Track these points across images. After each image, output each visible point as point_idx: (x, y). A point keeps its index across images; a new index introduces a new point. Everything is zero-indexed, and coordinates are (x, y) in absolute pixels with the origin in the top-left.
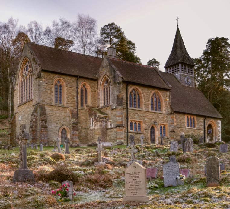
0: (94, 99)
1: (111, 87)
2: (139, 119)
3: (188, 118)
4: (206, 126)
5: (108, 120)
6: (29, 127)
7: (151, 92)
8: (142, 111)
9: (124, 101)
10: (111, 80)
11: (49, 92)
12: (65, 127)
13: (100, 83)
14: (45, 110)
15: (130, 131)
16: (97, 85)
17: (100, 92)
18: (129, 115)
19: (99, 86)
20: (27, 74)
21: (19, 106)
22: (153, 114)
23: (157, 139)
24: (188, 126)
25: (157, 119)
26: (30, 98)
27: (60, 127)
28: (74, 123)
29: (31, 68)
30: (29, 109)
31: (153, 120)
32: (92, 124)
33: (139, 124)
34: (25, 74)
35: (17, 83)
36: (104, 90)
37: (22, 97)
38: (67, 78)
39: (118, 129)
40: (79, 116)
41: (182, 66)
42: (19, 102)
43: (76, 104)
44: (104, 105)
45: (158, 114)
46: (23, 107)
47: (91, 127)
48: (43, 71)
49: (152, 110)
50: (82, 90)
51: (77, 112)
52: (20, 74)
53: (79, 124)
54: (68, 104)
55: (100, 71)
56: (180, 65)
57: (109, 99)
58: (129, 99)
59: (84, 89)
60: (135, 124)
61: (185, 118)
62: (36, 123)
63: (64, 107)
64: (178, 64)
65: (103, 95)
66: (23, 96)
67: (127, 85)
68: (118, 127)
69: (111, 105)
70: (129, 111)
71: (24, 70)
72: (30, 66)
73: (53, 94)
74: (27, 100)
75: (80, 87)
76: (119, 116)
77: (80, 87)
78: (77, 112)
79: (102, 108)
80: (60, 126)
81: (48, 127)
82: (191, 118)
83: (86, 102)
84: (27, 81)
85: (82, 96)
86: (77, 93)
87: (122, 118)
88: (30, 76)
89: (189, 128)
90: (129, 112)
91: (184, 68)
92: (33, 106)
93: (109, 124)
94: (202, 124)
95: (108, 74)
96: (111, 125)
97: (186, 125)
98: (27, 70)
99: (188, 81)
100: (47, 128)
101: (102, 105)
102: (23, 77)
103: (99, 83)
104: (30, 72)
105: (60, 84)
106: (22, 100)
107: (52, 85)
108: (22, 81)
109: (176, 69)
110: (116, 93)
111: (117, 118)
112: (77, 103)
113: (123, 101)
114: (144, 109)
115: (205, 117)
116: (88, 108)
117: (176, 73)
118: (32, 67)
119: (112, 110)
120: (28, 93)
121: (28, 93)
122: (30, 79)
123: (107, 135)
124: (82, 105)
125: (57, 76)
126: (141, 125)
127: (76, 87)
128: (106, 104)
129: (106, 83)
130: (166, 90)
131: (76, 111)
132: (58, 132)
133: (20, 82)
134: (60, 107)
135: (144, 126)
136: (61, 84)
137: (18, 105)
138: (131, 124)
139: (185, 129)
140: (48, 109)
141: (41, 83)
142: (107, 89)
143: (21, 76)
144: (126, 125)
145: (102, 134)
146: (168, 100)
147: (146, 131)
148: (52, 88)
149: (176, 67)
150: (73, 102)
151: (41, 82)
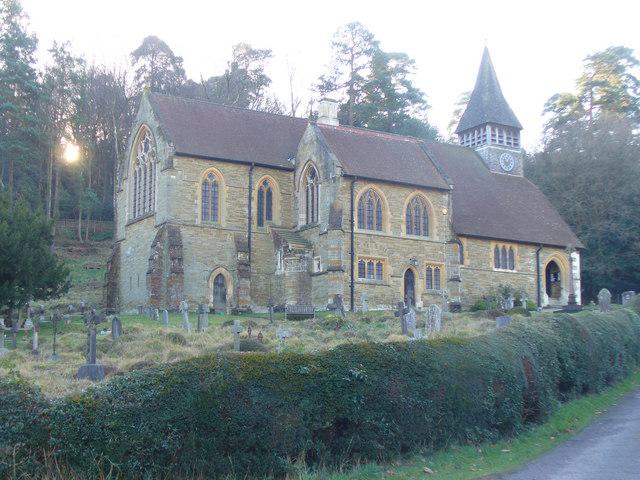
0: (290, 209)
3: (497, 251)
4: (543, 267)
5: (314, 255)
7: (406, 197)
9: (345, 217)
12: (223, 271)
14: (180, 237)
15: (357, 278)
17: (298, 195)
18: (355, 246)
19: (297, 183)
23: (418, 297)
25: (420, 253)
28: (241, 263)
30: (146, 232)
31: (411, 256)
33: (379, 265)
34: (143, 157)
38: (230, 168)
41: (493, 130)
46: (136, 227)
48: (178, 154)
49: (408, 233)
50: (260, 192)
51: (249, 238)
53: (252, 265)
55: (300, 152)
56: (489, 129)
57: (315, 212)
58: (356, 213)
59: (265, 189)
60: (370, 264)
61: (489, 248)
62: (161, 264)
64: (484, 126)
71: (139, 150)
73: (199, 201)
76: (332, 249)
77: (256, 187)
78: (249, 238)
79: (304, 228)
82: (504, 249)
83: (269, 217)
85: (260, 203)
86: (250, 198)
87: (340, 253)
89: (500, 270)
92: (156, 227)
93: (315, 263)
94: (533, 261)
95: (314, 159)
97: (492, 265)
98: (146, 151)
99: (507, 164)
101: (302, 223)
104: (153, 154)
110: (329, 200)
112: (250, 218)
113: (344, 217)
114: (390, 233)
115: (539, 246)
116: (273, 231)
118: (155, 146)
123: (311, 287)
124: (260, 223)
128: (310, 221)
129: (312, 178)
130: (443, 191)
133: (131, 174)
135: (388, 269)
138: (361, 265)
140: (186, 234)
142: (313, 189)
144: (348, 266)
145: (300, 286)
146: (445, 211)
147: (395, 279)
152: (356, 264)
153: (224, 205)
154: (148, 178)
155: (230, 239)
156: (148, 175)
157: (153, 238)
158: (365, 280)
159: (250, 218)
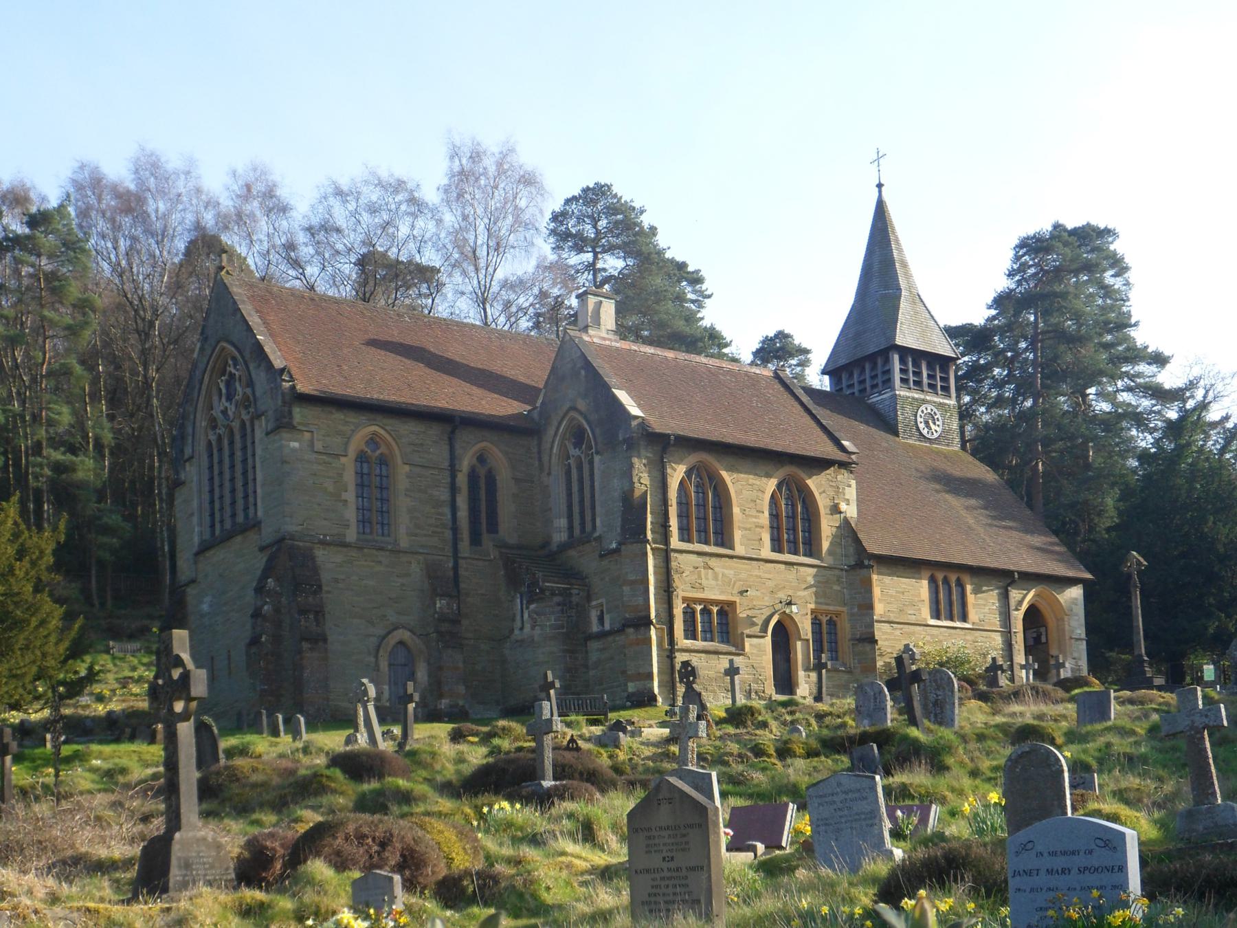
1: (597, 458)
2: (722, 593)
4: (1018, 616)
6: (247, 641)
8: (731, 557)
10: (598, 431)
11: (331, 488)
12: (405, 635)
13: (549, 446)
14: (315, 570)
15: (682, 641)
16: (539, 453)
19: (545, 458)
20: (230, 413)
21: (197, 554)
22: (783, 566)
24: (938, 617)
26: (246, 517)
27: (384, 638)
28: (443, 619)
29: (248, 386)
31: (782, 595)
32: (518, 617)
33: (722, 613)
35: (188, 451)
36: (568, 473)
37: (212, 515)
38: (408, 429)
39: (632, 637)
40: (462, 585)
42: (201, 533)
43: (448, 534)
44: (571, 535)
45: (802, 569)
46: (218, 555)
47: (517, 632)
50: (473, 477)
51: (456, 568)
52: (198, 416)
53: (465, 622)
54: (416, 535)
59: (482, 472)
60: (706, 611)
63: (399, 552)
65: (563, 495)
66: (217, 506)
67: (664, 450)
68: (631, 630)
69: (600, 537)
70: (678, 561)
71: (215, 398)
72: (244, 379)
74: (234, 524)
75: (465, 464)
76: (633, 583)
77: (465, 464)
78: (456, 568)
79: (564, 547)
80: (381, 632)
81: (330, 639)
83: (493, 527)
84: (232, 443)
86: (454, 489)
88: (243, 423)
90: (673, 564)
91: (911, 369)
92: (262, 549)
93: (594, 615)
96: (601, 619)
97: (925, 613)
98: (229, 399)
100: (325, 640)
101: (560, 537)
102: (214, 428)
103: (546, 446)
105: (378, 452)
106: (213, 526)
107: (343, 460)
108: (210, 443)
109: (874, 377)
111: (626, 589)
112: (455, 530)
117: (876, 390)
118: (250, 384)
119: (601, 556)
120: (240, 495)
121: (240, 495)
122: (244, 436)
124: (476, 539)
125: (362, 418)
126: (730, 615)
127: (446, 464)
128: (577, 532)
129: (578, 444)
131: (451, 565)
132: (373, 659)
133: (202, 447)
134: (382, 549)
136: (381, 454)
137: (195, 549)
138: (689, 615)
139: (922, 628)
141: (294, 450)
142: (580, 468)
143: (204, 424)
148: (344, 469)
149: (874, 367)
150: (437, 526)
151: (295, 445)
152: (678, 610)
153: (403, 504)
154: (239, 454)
155: (416, 568)
156: (238, 444)
157: (259, 573)
158: (699, 644)
159: (455, 530)
